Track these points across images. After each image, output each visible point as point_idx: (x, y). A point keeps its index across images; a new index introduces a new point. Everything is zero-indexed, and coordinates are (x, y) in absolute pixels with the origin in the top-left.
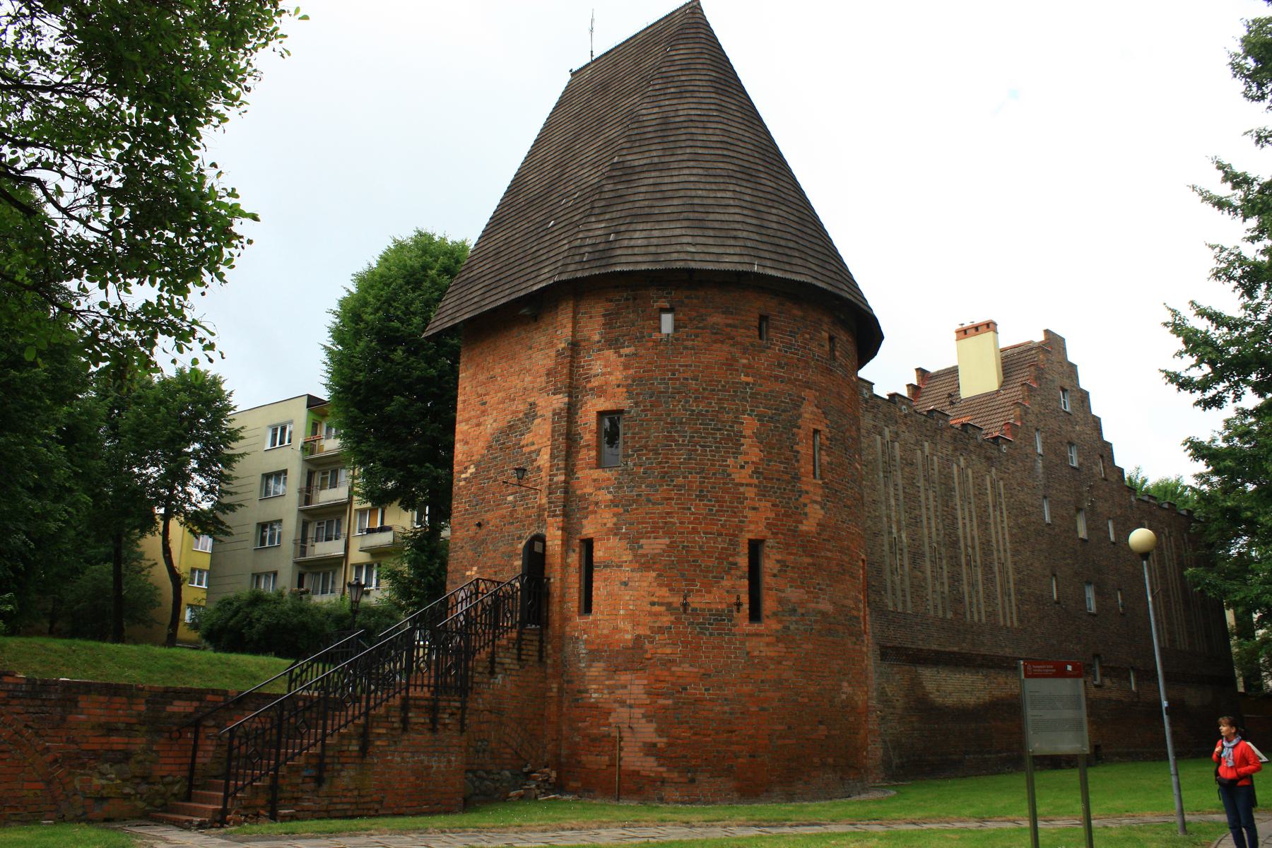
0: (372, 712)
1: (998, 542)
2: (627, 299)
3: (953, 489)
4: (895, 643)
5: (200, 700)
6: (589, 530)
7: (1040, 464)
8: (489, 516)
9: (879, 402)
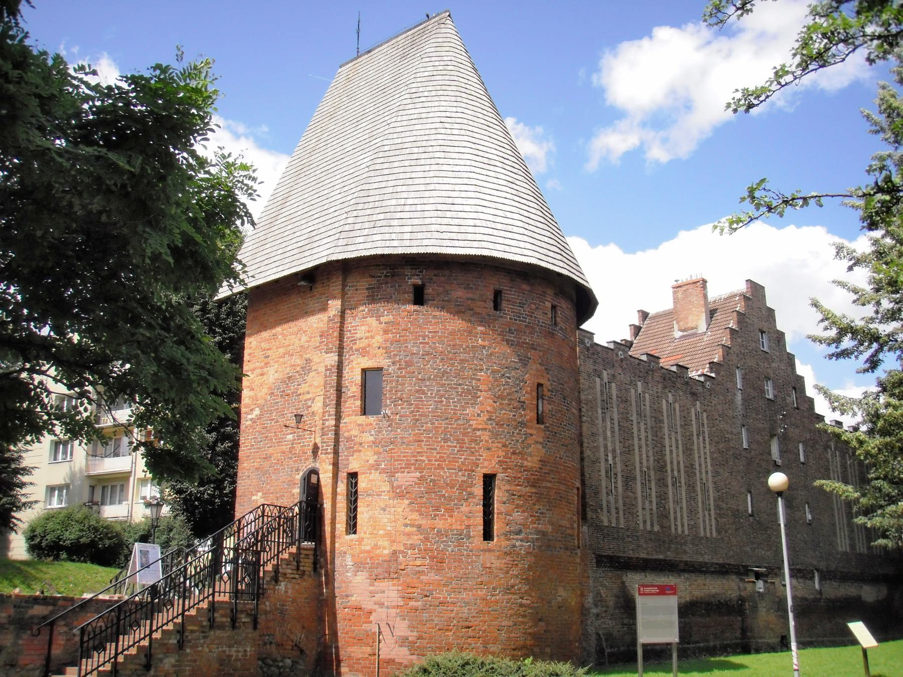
0: (187, 613)
1: (700, 465)
2: (386, 276)
3: (662, 421)
4: (610, 553)
5: (54, 605)
6: (354, 465)
7: (739, 397)
9: (599, 349)
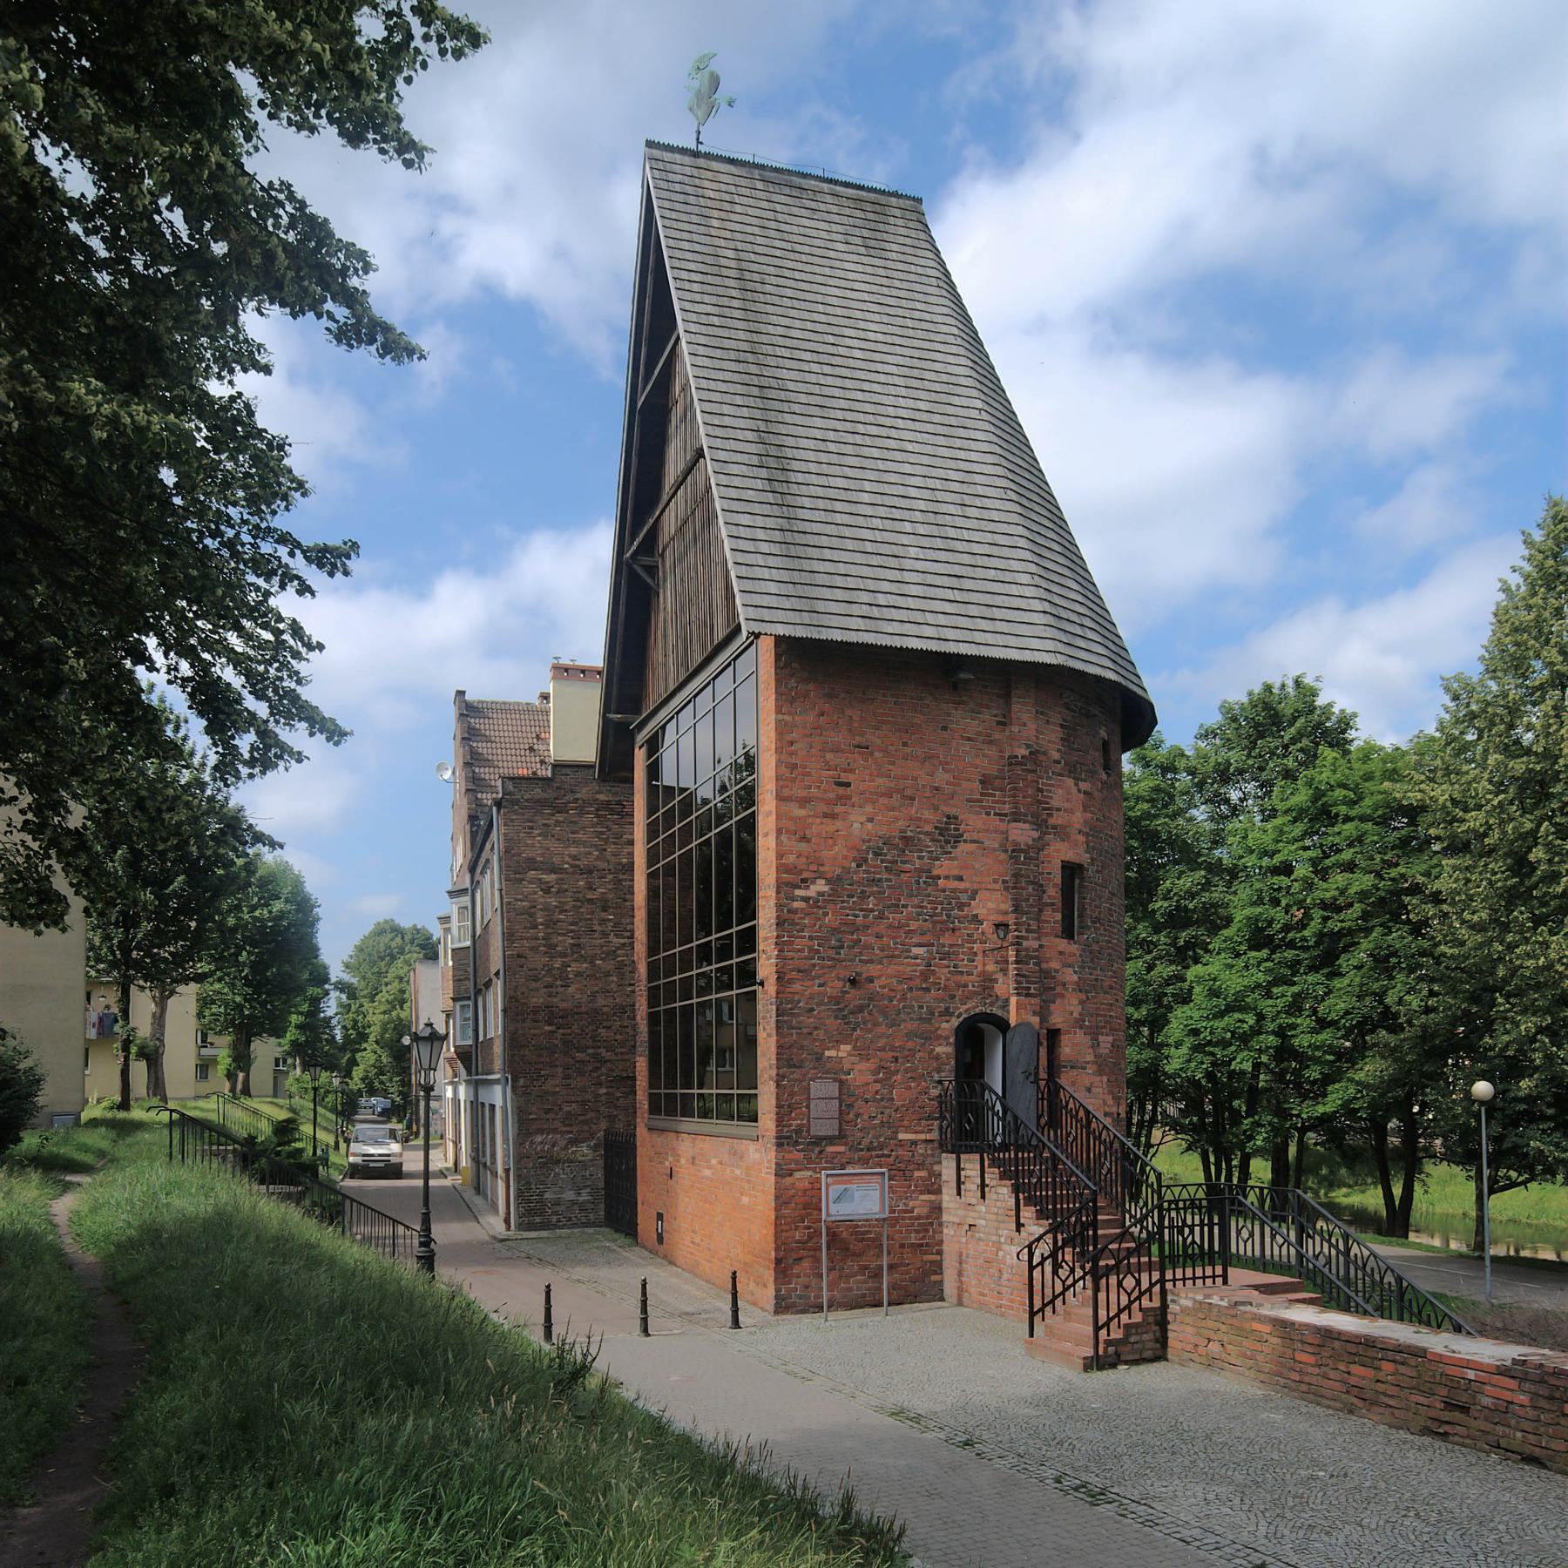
6: (1057, 1019)
8: (873, 970)
